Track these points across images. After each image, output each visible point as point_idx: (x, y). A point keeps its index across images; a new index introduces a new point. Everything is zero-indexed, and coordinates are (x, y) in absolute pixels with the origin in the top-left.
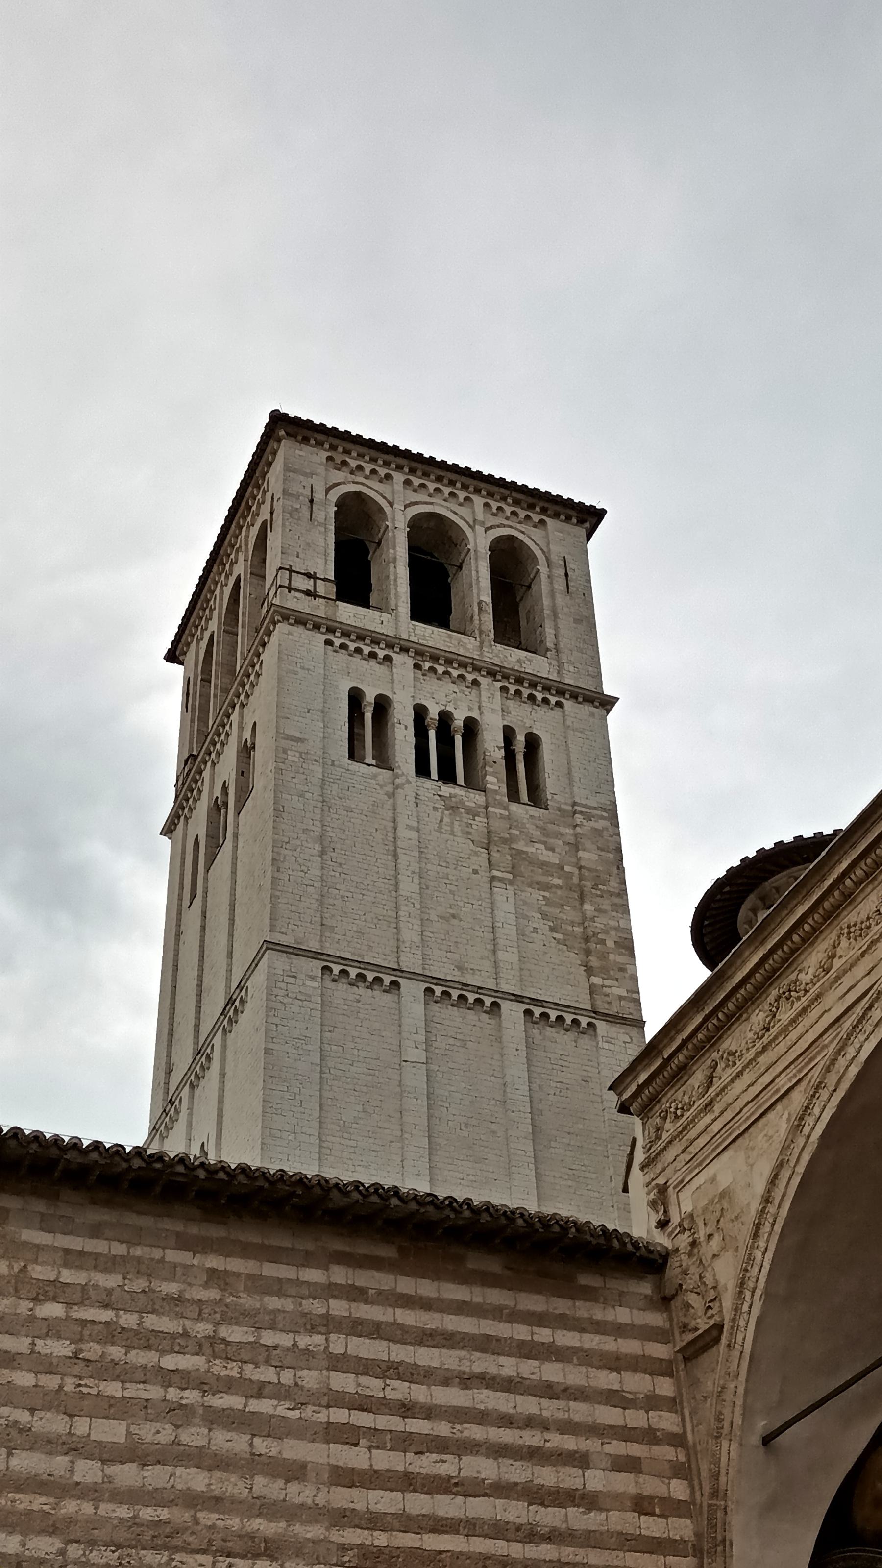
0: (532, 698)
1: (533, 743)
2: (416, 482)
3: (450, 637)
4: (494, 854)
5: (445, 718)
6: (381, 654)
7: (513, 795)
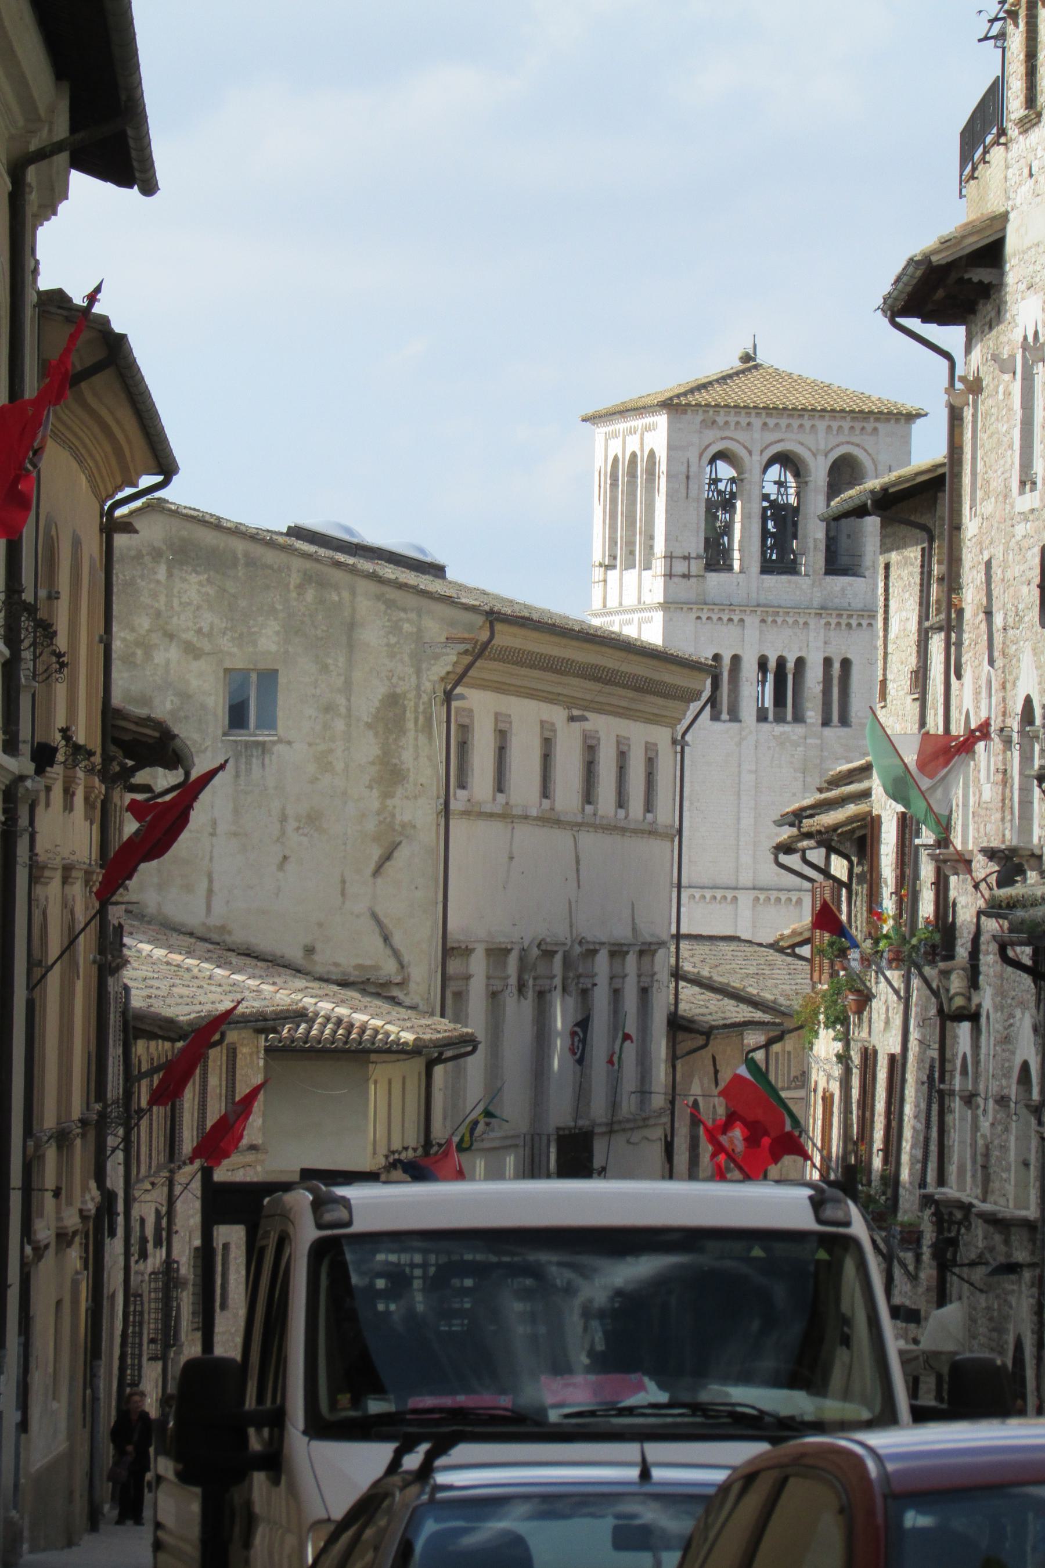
0: (849, 625)
1: (846, 663)
2: (771, 422)
3: (789, 582)
4: (809, 779)
5: (781, 662)
6: (736, 618)
7: (826, 722)
